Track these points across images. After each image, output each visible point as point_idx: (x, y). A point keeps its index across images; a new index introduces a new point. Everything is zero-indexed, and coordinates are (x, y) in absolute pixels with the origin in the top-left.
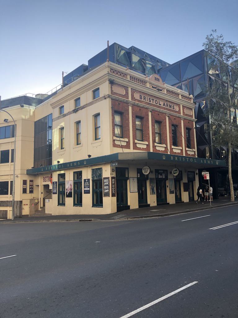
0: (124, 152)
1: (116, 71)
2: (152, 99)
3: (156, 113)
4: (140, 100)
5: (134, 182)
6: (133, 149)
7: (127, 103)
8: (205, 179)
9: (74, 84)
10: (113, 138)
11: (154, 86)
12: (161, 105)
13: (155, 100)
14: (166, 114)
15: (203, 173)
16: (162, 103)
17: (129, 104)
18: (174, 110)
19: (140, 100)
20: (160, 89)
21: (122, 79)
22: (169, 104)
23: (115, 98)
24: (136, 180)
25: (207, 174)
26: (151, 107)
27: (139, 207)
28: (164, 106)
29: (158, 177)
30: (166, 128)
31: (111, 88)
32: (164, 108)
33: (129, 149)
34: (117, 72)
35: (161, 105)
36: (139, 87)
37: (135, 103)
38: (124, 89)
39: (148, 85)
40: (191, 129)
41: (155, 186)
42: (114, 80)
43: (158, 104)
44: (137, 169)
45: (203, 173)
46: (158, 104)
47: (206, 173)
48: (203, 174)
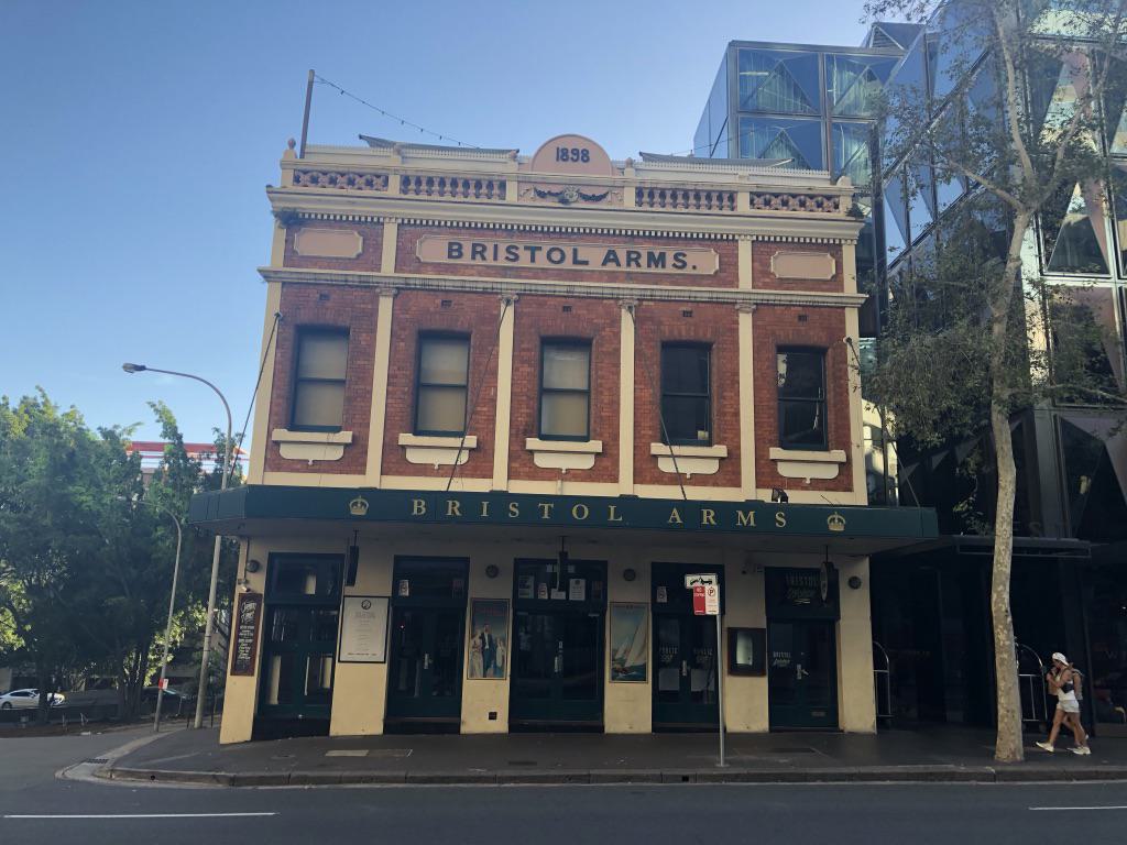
0: (678, 488)
1: (343, 175)
2: (526, 248)
3: (551, 302)
4: (452, 261)
5: (373, 616)
6: (757, 487)
7: (370, 290)
8: (697, 612)
9: (792, 292)
10: (269, 434)
11: (589, 192)
12: (586, 263)
13: (546, 249)
14: (618, 299)
15: (689, 579)
16: (594, 255)
17: (378, 290)
18: (688, 270)
19: (452, 261)
20: (598, 193)
21: (688, 214)
22: (644, 250)
23: (834, 300)
24: (381, 611)
25: (707, 587)
26: (514, 284)
27: (654, 729)
28: (611, 267)
29: (536, 595)
30: (618, 365)
31: (289, 242)
32: (613, 277)
33: (737, 489)
34: (768, 196)
35: (586, 263)
36: (445, 209)
37: (465, 281)
38: (356, 233)
39: (512, 194)
40: (822, 351)
41: (504, 640)
42: (295, 209)
43: (568, 264)
44: (398, 560)
45: (689, 579)
46: (568, 264)
47: (705, 578)
48: (688, 585)
